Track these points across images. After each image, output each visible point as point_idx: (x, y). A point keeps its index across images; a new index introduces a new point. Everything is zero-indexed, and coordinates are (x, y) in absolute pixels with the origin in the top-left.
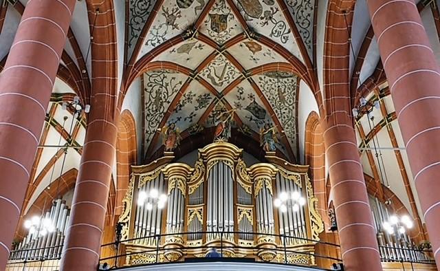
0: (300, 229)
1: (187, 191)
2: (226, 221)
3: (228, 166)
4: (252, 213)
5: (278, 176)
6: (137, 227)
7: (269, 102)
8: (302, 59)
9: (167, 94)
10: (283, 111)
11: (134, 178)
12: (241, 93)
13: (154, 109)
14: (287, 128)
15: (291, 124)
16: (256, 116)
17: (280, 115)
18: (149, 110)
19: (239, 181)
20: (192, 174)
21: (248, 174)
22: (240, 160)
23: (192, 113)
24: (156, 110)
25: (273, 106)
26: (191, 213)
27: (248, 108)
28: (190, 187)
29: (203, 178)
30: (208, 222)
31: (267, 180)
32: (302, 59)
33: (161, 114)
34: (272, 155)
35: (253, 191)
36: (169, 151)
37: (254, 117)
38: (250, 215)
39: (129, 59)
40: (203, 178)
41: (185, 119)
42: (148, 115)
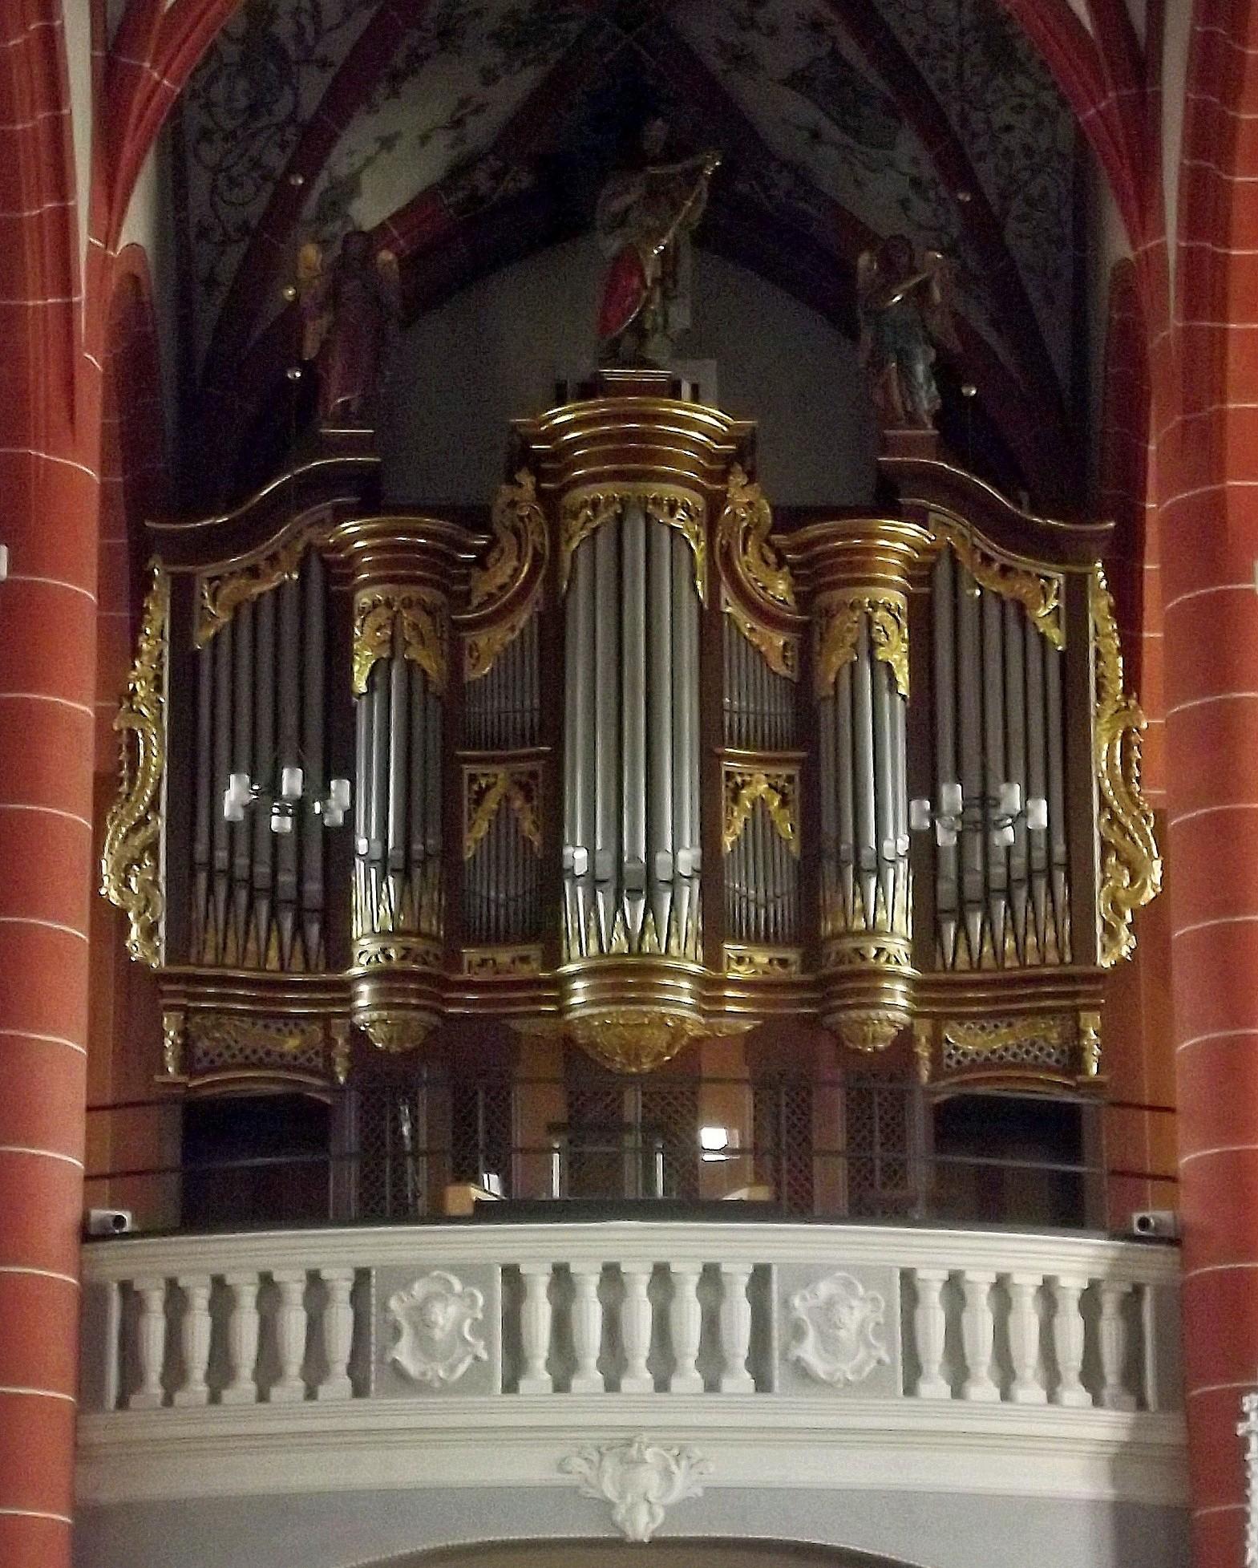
0: (1041, 885)
1: (456, 668)
2: (663, 858)
3: (672, 528)
4: (795, 792)
5: (943, 572)
6: (202, 879)
7: (922, 65)
9: (316, 13)
10: (1002, 116)
11: (161, 587)
13: (242, 102)
14: (1022, 219)
15: (1044, 194)
16: (845, 128)
17: (982, 144)
18: (208, 106)
19: (731, 608)
20: (481, 563)
21: (781, 562)
22: (738, 479)
23: (463, 103)
24: (253, 110)
25: (944, 86)
26: (481, 794)
27: (798, 81)
28: (469, 637)
29: (538, 589)
30: (568, 851)
31: (880, 615)
33: (280, 127)
34: (908, 446)
35: (806, 654)
36: (344, 418)
37: (832, 131)
38: (784, 803)
40: (538, 589)
41: (424, 139)
42: (205, 135)
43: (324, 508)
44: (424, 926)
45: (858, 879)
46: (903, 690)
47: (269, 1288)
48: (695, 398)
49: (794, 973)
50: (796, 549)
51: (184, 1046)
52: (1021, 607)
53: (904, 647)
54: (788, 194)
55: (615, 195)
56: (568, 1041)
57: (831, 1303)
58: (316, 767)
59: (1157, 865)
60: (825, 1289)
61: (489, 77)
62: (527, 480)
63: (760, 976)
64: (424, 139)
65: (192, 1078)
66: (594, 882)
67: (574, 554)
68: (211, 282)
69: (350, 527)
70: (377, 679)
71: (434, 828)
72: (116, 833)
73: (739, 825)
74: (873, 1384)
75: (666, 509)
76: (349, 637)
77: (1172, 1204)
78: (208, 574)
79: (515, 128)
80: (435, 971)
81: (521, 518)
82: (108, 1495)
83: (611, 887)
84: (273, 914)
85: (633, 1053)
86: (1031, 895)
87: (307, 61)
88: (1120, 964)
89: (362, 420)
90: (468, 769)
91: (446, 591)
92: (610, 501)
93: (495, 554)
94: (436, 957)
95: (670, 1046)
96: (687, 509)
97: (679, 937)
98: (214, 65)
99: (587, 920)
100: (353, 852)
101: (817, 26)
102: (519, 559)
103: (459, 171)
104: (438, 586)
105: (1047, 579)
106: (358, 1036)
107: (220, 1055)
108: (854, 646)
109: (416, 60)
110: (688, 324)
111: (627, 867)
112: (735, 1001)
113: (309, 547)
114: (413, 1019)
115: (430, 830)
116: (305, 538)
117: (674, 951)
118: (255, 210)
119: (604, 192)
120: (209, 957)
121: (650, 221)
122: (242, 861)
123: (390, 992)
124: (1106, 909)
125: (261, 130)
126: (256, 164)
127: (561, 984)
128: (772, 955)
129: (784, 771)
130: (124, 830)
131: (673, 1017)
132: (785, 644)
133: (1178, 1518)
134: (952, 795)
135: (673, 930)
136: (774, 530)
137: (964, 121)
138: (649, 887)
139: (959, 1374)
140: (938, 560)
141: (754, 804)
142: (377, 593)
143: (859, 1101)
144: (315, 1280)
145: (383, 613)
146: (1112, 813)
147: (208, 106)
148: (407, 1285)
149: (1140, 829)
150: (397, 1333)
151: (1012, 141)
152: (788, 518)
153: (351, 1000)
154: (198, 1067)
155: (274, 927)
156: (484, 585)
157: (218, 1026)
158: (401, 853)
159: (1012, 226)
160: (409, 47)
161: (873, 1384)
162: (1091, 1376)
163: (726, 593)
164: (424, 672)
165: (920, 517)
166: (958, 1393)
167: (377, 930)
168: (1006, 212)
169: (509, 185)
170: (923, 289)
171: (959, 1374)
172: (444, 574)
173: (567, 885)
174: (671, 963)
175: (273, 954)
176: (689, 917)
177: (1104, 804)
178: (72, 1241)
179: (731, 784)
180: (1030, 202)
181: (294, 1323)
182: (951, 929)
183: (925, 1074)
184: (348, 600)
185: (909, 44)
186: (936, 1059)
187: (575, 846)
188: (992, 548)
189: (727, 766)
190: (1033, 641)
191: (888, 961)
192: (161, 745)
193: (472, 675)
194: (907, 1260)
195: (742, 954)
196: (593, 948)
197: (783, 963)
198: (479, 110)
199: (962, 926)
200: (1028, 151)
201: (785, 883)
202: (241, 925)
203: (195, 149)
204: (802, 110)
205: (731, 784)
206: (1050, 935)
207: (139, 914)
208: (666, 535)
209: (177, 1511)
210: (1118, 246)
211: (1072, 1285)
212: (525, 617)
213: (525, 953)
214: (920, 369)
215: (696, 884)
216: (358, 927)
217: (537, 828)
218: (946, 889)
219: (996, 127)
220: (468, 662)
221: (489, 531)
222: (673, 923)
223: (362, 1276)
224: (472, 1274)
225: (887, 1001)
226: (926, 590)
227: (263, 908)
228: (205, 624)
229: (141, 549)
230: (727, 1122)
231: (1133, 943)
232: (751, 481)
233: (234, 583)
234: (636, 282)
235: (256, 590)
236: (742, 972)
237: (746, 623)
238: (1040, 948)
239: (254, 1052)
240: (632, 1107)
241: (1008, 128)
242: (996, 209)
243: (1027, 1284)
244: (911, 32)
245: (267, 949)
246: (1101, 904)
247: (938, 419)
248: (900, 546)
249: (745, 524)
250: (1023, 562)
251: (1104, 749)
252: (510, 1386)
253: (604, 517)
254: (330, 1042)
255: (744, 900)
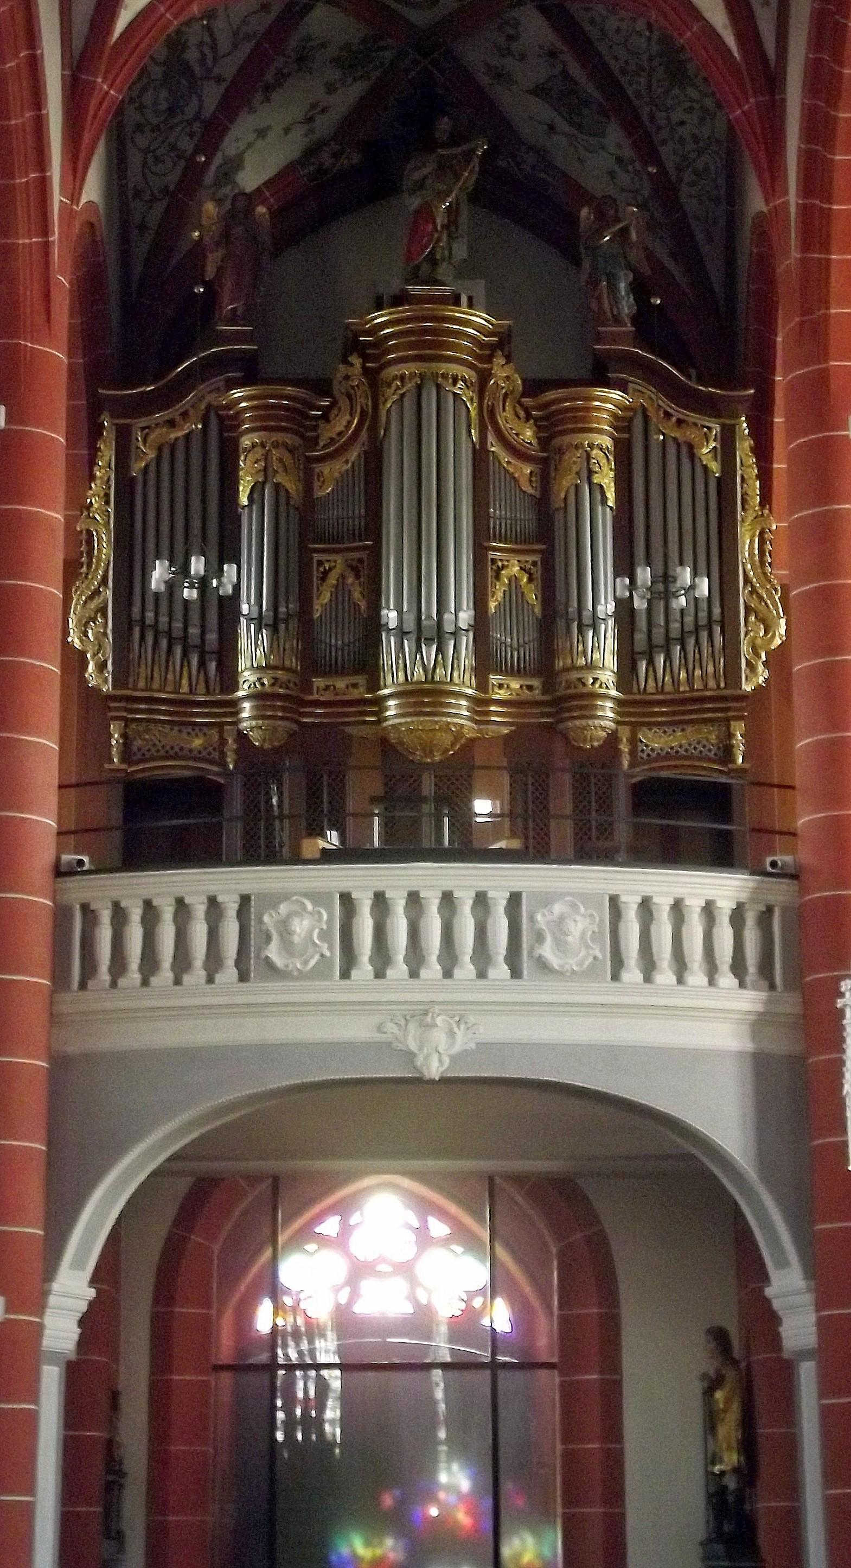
0: (704, 635)
2: (448, 617)
3: (455, 394)
4: (538, 572)
5: (638, 422)
6: (137, 631)
7: (624, 80)
8: (730, 40)
9: (214, 45)
10: (677, 116)
11: (109, 434)
12: (510, 38)
13: (164, 106)
14: (692, 184)
15: (706, 168)
16: (571, 123)
17: (664, 134)
18: (141, 108)
19: (494, 447)
20: (325, 417)
21: (528, 417)
22: (499, 360)
23: (313, 106)
24: (171, 110)
25: (638, 95)
26: (325, 574)
27: (540, 91)
28: (317, 467)
29: (364, 435)
30: (384, 612)
31: (595, 452)
32: (730, 40)
33: (189, 123)
34: (615, 338)
35: (545, 479)
36: (233, 319)
38: (530, 580)
39: (78, 43)
40: (364, 435)
41: (287, 131)
42: (139, 128)
43: (219, 380)
44: (287, 663)
45: (581, 631)
46: (611, 503)
47: (182, 908)
48: (470, 306)
49: (537, 695)
50: (538, 408)
51: (125, 744)
52: (691, 447)
53: (612, 474)
54: (533, 168)
55: (416, 168)
56: (384, 741)
57: (562, 919)
58: (214, 555)
59: (783, 622)
60: (558, 908)
61: (331, 89)
62: (356, 361)
63: (514, 697)
64: (287, 131)
65: (130, 766)
66: (402, 633)
67: (389, 412)
68: (143, 227)
69: (237, 393)
70: (255, 496)
71: (294, 597)
72: (78, 600)
73: (500, 595)
74: (590, 973)
75: (451, 381)
76: (236, 467)
77: (793, 851)
78: (141, 425)
79: (349, 123)
80: (294, 693)
81: (353, 387)
82: (73, 1048)
83: (413, 637)
84: (185, 654)
85: (428, 749)
86: (697, 642)
87: (208, 78)
88: (758, 689)
89: (245, 321)
90: (317, 557)
91: (302, 436)
92: (413, 375)
93: (335, 412)
94: (295, 684)
95: (453, 744)
96: (465, 381)
97: (459, 671)
98: (145, 80)
99: (397, 659)
100: (239, 613)
101: (552, 54)
102: (351, 415)
103: (310, 152)
104: (296, 433)
105: (709, 428)
106: (242, 737)
107: (149, 750)
108: (577, 473)
109: (282, 77)
110: (465, 255)
111: (424, 623)
112: (497, 714)
113: (209, 406)
114: (279, 726)
115: (291, 598)
116: (206, 400)
117: (456, 680)
118: (173, 178)
119: (409, 166)
120: (142, 684)
121: (440, 186)
122: (164, 619)
123: (264, 707)
124: (748, 651)
125: (177, 125)
126: (173, 147)
127: (380, 702)
128: (522, 682)
129: (531, 558)
130: (84, 598)
131: (455, 724)
132: (531, 473)
133: (797, 1063)
134: (644, 574)
135: (455, 666)
136: (524, 395)
137: (652, 118)
138: (439, 637)
139: (649, 966)
140: (635, 415)
141: (510, 581)
142: (255, 438)
143: (581, 781)
144: (213, 902)
145: (259, 452)
146: (753, 586)
147: (141, 108)
148: (275, 906)
149: (771, 597)
150: (268, 938)
151: (684, 132)
152: (533, 387)
153: (237, 713)
154: (134, 758)
155: (186, 664)
156: (328, 432)
157: (147, 731)
158: (271, 614)
159: (684, 190)
160: (276, 68)
161: (590, 973)
162: (738, 968)
163: (491, 438)
164: (287, 491)
165: (622, 386)
166: (648, 979)
167: (255, 666)
168: (680, 180)
169: (344, 162)
170: (624, 232)
171: (649, 966)
172: (300, 425)
173: (384, 635)
174: (454, 688)
175: (185, 682)
176: (466, 657)
177: (747, 580)
178: (48, 876)
179: (494, 567)
180: (697, 173)
181: (199, 932)
182: (643, 665)
183: (626, 763)
184: (236, 442)
185: (615, 66)
186: (633, 753)
187: (389, 609)
188: (671, 408)
189: (492, 554)
190: (699, 470)
191: (601, 687)
192: (109, 540)
193: (319, 493)
194: (614, 889)
195: (502, 682)
196: (401, 678)
197: (530, 688)
198: (324, 110)
199: (651, 663)
200: (696, 139)
201: (531, 634)
202: (163, 662)
203: (132, 138)
204: (543, 110)
205: (494, 567)
206: (711, 669)
207: (94, 655)
208: (451, 397)
209: (120, 1059)
210: (756, 202)
211: (725, 906)
212: (355, 454)
213: (355, 681)
214: (622, 286)
215: (471, 635)
216: (242, 664)
217: (364, 597)
218: (640, 638)
219: (674, 122)
220: (316, 484)
221: (331, 396)
222: (456, 661)
223: (245, 900)
224: (319, 898)
225: (600, 713)
226: (626, 436)
227: (178, 651)
228: (138, 459)
229: (95, 407)
230: (491, 796)
231: (766, 674)
232: (508, 362)
233: (158, 431)
234: (430, 228)
235: (173, 436)
236: (502, 694)
237: (505, 458)
238: (704, 678)
239: (172, 748)
240: (428, 786)
241: (682, 123)
242: (673, 178)
243: (694, 905)
244: (616, 58)
245: (181, 678)
246: (745, 648)
247: (635, 320)
248: (609, 406)
249: (504, 391)
250: (692, 417)
251: (747, 543)
252: (345, 975)
253: (409, 386)
254: (223, 742)
255: (503, 646)
